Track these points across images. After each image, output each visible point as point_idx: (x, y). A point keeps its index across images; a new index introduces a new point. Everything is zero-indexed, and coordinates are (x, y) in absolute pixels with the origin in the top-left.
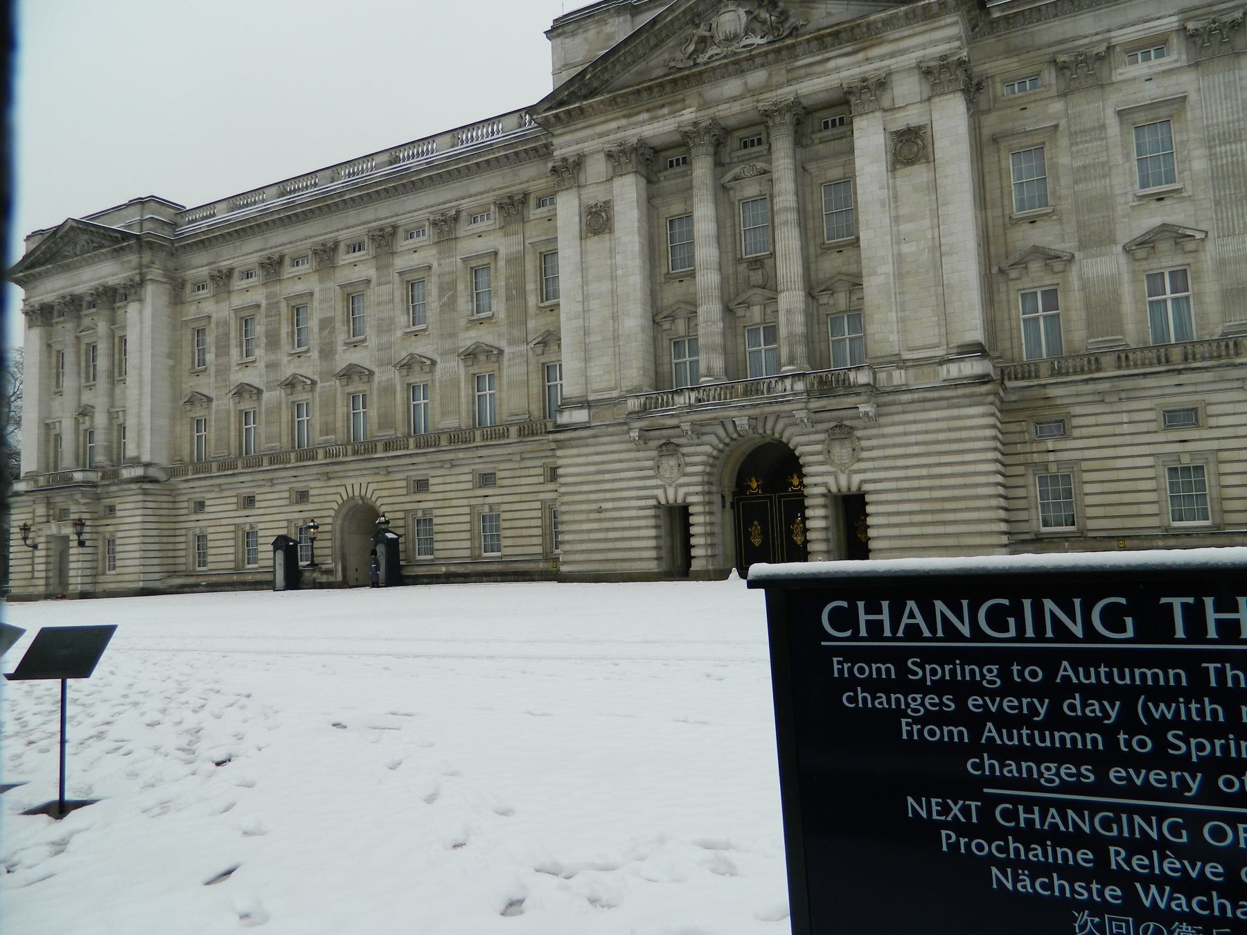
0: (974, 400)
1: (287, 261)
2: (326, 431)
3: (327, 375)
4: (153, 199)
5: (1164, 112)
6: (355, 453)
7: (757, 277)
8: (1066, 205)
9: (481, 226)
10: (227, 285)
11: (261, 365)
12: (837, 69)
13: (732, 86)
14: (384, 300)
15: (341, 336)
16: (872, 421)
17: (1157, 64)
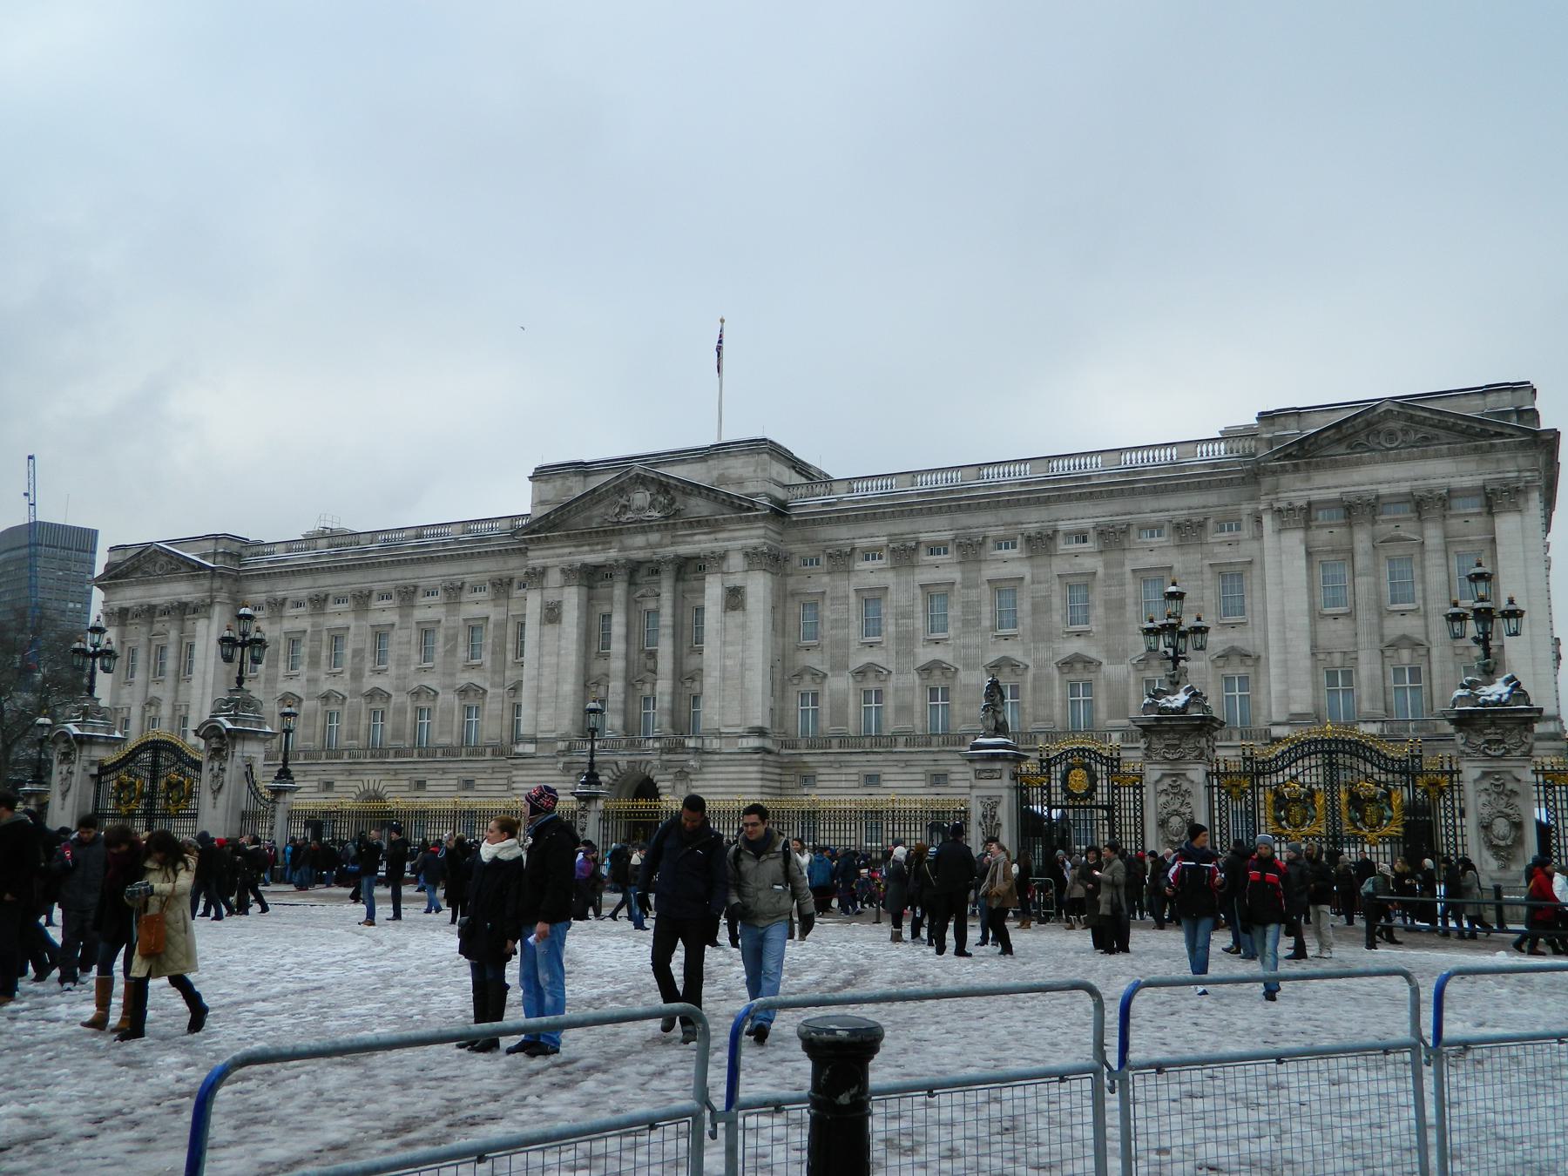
0: (751, 763)
1: (331, 598)
2: (352, 736)
3: (355, 693)
4: (226, 537)
5: (877, 594)
6: (373, 756)
7: (650, 664)
8: (826, 642)
9: (479, 595)
10: (280, 611)
11: (303, 679)
12: (699, 542)
13: (639, 540)
14: (403, 642)
15: (368, 665)
16: (699, 771)
17: (878, 563)
